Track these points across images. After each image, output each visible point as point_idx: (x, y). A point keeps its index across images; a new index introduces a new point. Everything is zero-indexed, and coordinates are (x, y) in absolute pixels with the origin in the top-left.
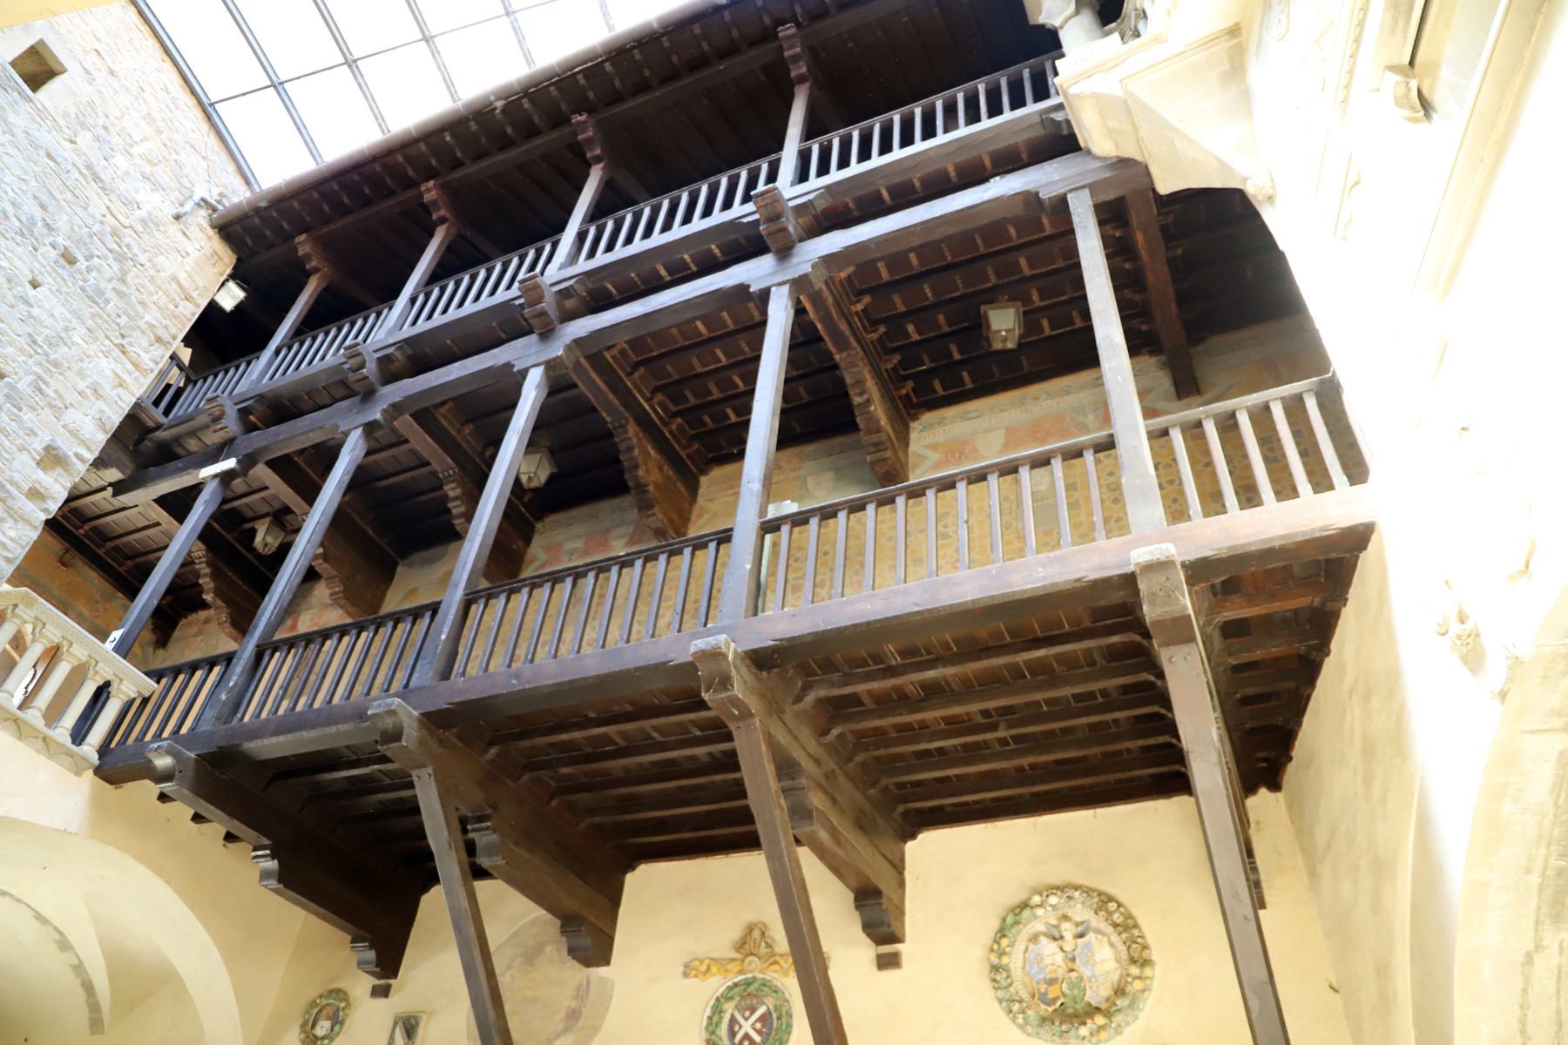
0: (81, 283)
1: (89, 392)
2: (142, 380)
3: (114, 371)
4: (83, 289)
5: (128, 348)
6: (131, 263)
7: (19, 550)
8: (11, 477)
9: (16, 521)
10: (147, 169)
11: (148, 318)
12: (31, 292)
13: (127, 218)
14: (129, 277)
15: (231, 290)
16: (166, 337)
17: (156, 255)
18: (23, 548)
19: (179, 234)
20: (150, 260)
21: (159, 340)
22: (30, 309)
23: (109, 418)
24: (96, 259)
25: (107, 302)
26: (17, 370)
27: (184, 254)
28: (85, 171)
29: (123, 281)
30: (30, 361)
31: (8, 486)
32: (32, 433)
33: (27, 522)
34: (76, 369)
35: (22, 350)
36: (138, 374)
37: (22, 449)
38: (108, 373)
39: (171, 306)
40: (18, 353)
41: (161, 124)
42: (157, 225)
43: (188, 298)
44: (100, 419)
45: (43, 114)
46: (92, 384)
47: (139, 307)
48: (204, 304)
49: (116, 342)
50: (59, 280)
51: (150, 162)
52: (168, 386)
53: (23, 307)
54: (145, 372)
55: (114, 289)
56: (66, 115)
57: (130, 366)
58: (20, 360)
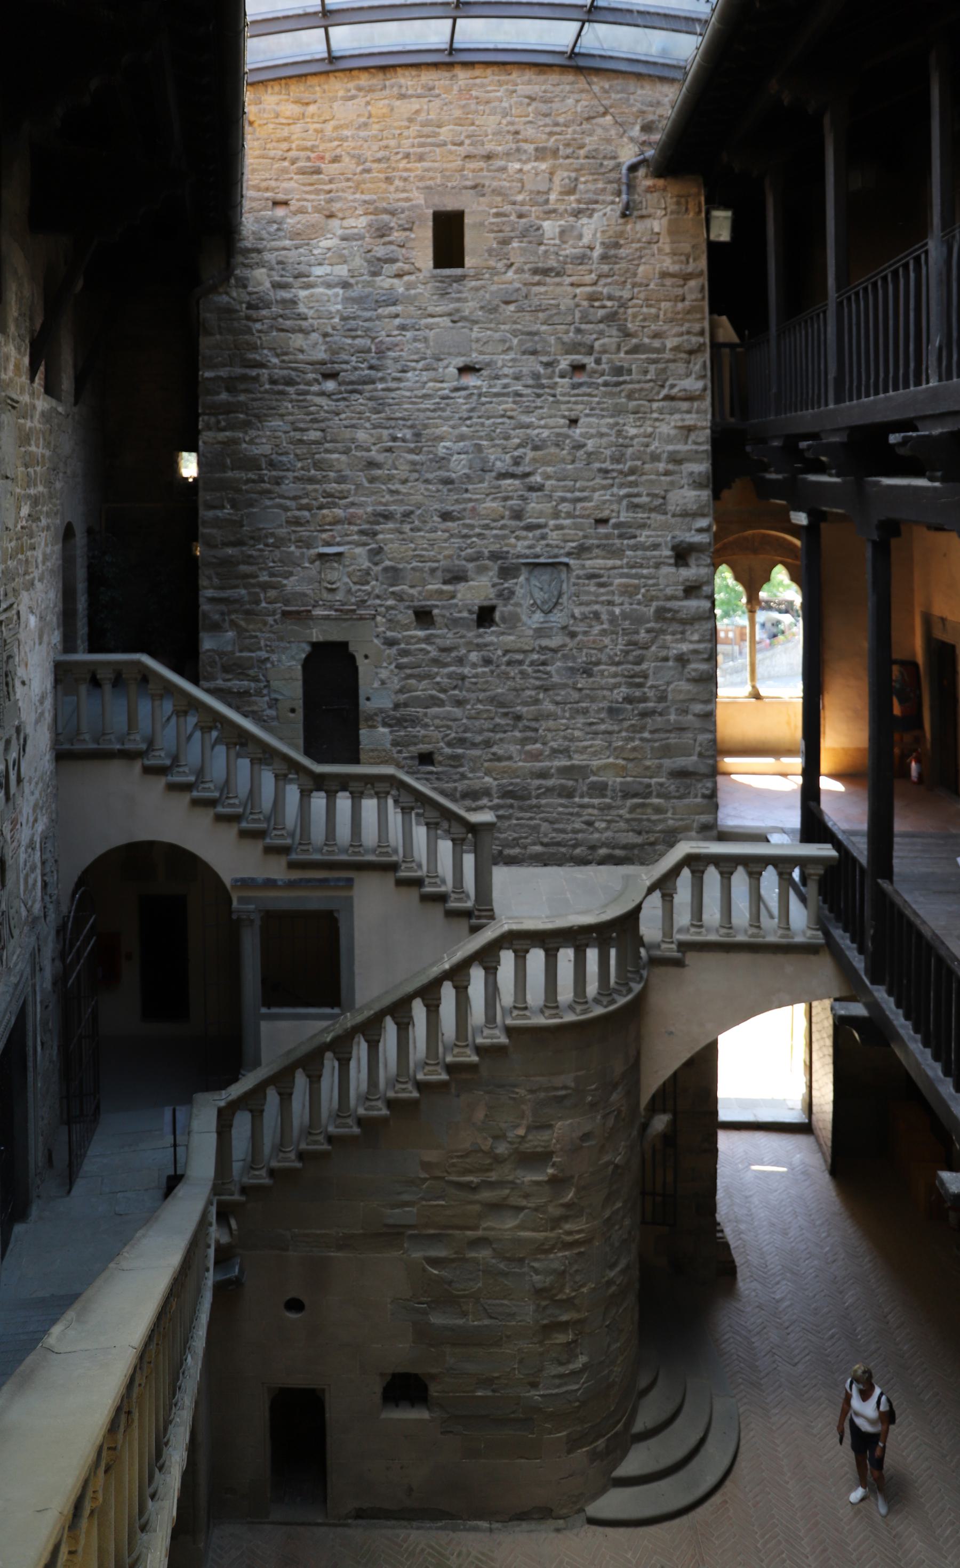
1: (671, 467)
3: (676, 427)
4: (606, 384)
6: (622, 310)
8: (666, 595)
11: (670, 343)
12: (577, 432)
13: (591, 272)
15: (718, 217)
17: (635, 275)
20: (634, 285)
21: (691, 352)
24: (597, 345)
25: (630, 372)
26: (612, 507)
28: (537, 278)
29: (628, 335)
30: (615, 490)
31: (669, 604)
32: (656, 546)
34: (648, 458)
36: (696, 404)
37: (657, 566)
38: (673, 432)
39: (680, 306)
40: (602, 492)
41: (551, 143)
42: (617, 245)
43: (687, 277)
44: (694, 482)
46: (668, 457)
47: (657, 344)
49: (661, 396)
53: (580, 453)
54: (700, 398)
55: (627, 353)
56: (490, 251)
57: (685, 405)
58: (608, 497)
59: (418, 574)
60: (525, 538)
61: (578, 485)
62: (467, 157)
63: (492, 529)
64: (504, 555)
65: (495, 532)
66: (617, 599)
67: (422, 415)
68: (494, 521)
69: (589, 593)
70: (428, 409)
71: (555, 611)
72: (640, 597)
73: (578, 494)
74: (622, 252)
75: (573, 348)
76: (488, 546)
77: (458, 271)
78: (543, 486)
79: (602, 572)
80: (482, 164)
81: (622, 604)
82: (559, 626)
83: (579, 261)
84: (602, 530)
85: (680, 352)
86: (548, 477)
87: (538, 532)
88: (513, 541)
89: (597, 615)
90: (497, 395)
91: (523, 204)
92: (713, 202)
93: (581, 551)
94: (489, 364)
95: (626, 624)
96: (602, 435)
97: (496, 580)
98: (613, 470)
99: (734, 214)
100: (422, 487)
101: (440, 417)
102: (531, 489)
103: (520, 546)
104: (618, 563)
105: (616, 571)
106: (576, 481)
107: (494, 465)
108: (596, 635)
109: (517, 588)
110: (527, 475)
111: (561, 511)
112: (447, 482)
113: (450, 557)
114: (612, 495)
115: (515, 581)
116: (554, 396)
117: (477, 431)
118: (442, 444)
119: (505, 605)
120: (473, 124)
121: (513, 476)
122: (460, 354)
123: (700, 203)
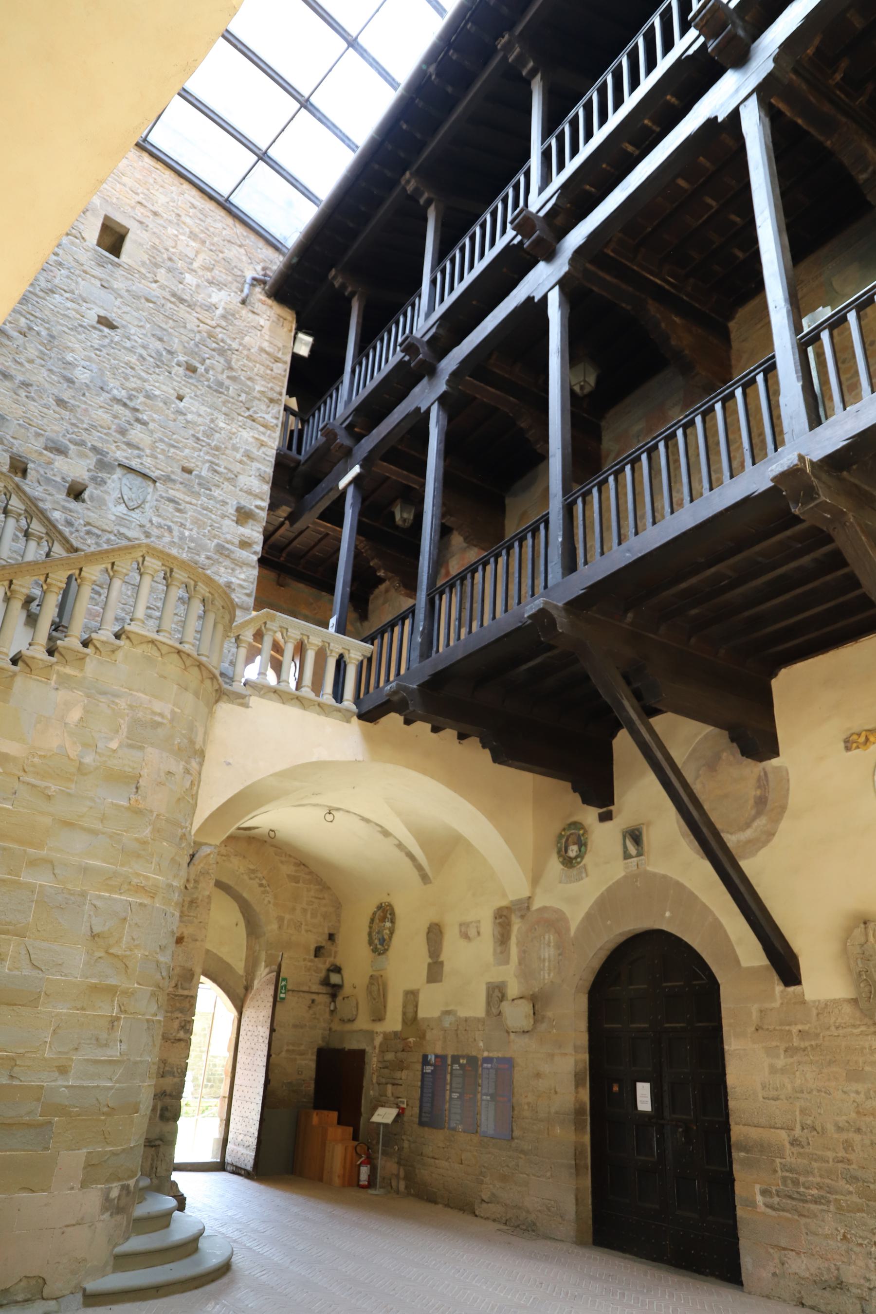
0: (206, 383)
2: (273, 435)
3: (253, 437)
4: (209, 387)
5: (256, 416)
6: (229, 352)
7: (251, 586)
8: (225, 538)
9: (241, 567)
10: (208, 275)
11: (258, 388)
14: (233, 363)
16: (275, 396)
17: (243, 338)
18: (253, 583)
19: (250, 315)
21: (272, 400)
22: (186, 417)
23: (265, 472)
24: (208, 361)
25: (228, 388)
26: (197, 463)
27: (260, 328)
28: (173, 299)
29: (230, 368)
30: (202, 454)
31: (227, 546)
33: (248, 565)
34: (230, 446)
35: (193, 448)
36: (269, 432)
37: (223, 516)
38: (251, 440)
39: (269, 372)
40: (192, 451)
42: (233, 315)
43: (277, 360)
45: (130, 270)
46: (244, 452)
47: (249, 383)
48: (288, 359)
50: (193, 387)
51: (210, 270)
52: (292, 432)
53: (181, 418)
55: (228, 377)
56: (143, 264)
57: (262, 429)
59: (23, 431)
60: (124, 450)
61: (175, 437)
62: (139, 203)
63: (98, 431)
64: (104, 453)
65: (99, 434)
66: (188, 525)
67: (60, 327)
68: (102, 427)
69: (168, 511)
70: (67, 327)
71: (137, 511)
72: (206, 531)
73: (172, 442)
74: (235, 322)
75: (192, 353)
76: (93, 439)
77: (116, 259)
78: (148, 423)
79: (181, 502)
80: (149, 214)
81: (191, 530)
82: (139, 523)
83: (206, 308)
84: (186, 475)
85: (265, 396)
86: (154, 420)
87: (136, 452)
88: (113, 447)
89: (170, 530)
90: (125, 348)
91: (173, 254)
92: (301, 327)
93: (168, 479)
94: (124, 327)
95: (193, 545)
96: (200, 415)
97: (92, 467)
98: (203, 441)
99: (314, 340)
100: (45, 373)
101: (74, 336)
102: (138, 420)
103: (121, 454)
104: (194, 501)
105: (191, 506)
106: (174, 434)
107: (111, 389)
108: (166, 543)
109: (109, 481)
110: (137, 410)
111: (157, 447)
112: (70, 381)
113: (57, 432)
114: (199, 456)
115: (109, 476)
116: (170, 373)
117: (104, 362)
118: (71, 354)
119: (96, 489)
120: (148, 190)
121: (125, 405)
122: (101, 307)
123: (292, 327)
